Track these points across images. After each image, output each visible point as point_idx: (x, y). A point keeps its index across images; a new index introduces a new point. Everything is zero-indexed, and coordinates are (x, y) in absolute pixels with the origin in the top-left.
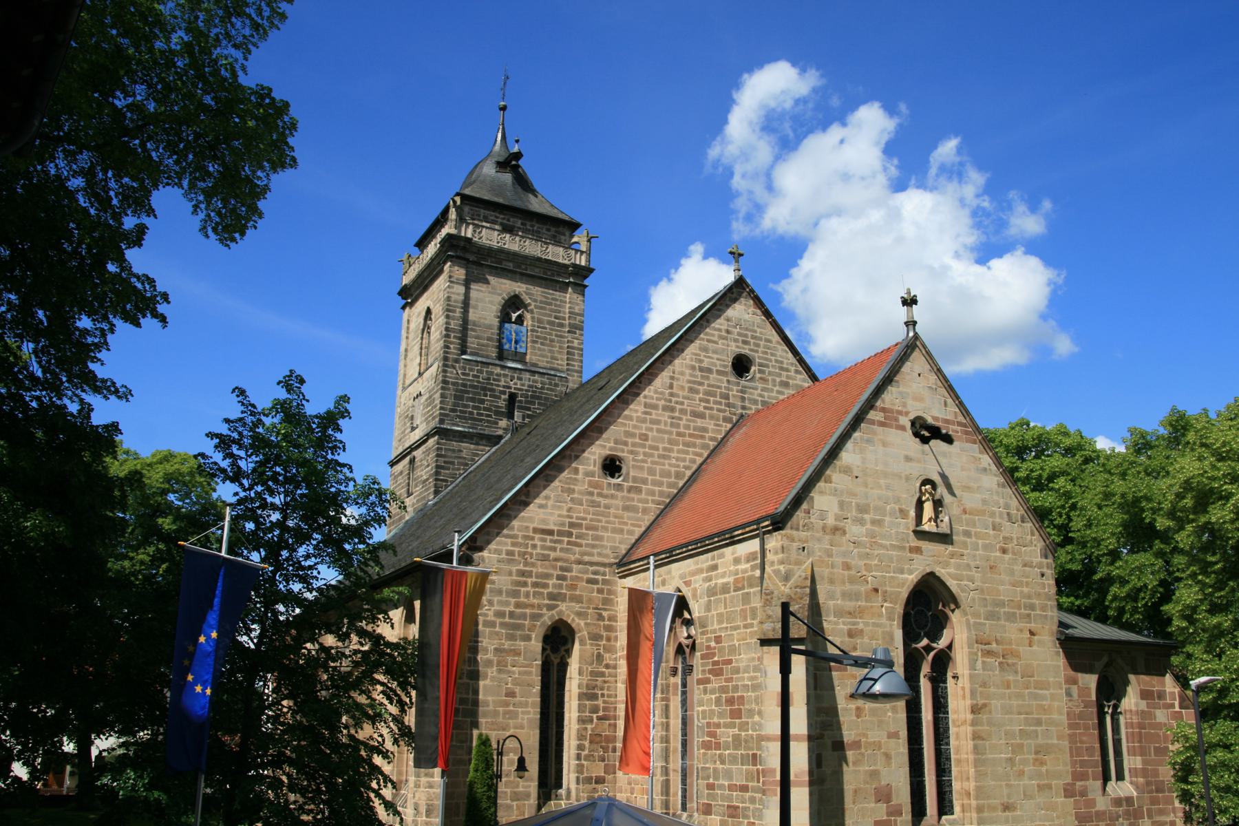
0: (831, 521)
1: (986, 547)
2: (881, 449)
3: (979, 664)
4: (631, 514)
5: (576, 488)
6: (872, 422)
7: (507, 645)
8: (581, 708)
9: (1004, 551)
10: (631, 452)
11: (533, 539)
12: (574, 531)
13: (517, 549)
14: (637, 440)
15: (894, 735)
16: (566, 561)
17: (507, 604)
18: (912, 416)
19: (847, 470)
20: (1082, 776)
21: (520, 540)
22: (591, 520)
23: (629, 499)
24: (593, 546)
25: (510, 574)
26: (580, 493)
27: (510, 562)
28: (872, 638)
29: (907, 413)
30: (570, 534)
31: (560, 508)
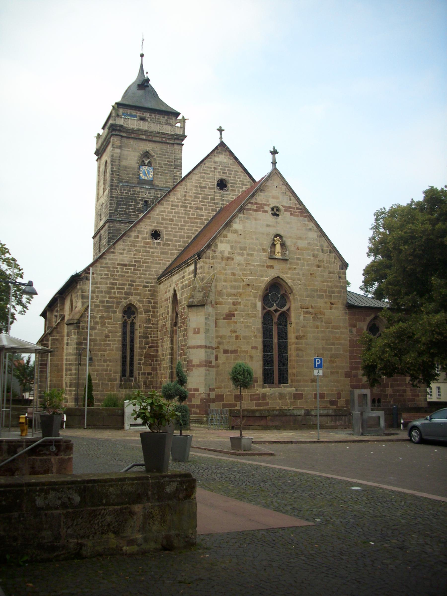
0: (226, 254)
1: (308, 265)
2: (254, 222)
3: (302, 318)
4: (165, 256)
5: (138, 245)
6: (250, 210)
7: (105, 315)
8: (140, 342)
9: (319, 266)
10: (165, 228)
11: (117, 268)
12: (137, 264)
13: (109, 273)
14: (168, 222)
15: (255, 348)
16: (133, 277)
17: (105, 297)
18: (272, 206)
19: (236, 232)
20: (357, 368)
21: (111, 269)
22: (145, 259)
23: (163, 249)
24: (146, 271)
25: (107, 284)
26: (140, 247)
27: (106, 279)
28: (245, 306)
29: (269, 205)
30: (135, 266)
31: (130, 254)
